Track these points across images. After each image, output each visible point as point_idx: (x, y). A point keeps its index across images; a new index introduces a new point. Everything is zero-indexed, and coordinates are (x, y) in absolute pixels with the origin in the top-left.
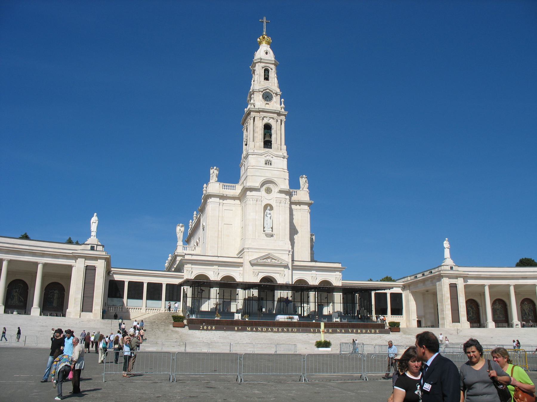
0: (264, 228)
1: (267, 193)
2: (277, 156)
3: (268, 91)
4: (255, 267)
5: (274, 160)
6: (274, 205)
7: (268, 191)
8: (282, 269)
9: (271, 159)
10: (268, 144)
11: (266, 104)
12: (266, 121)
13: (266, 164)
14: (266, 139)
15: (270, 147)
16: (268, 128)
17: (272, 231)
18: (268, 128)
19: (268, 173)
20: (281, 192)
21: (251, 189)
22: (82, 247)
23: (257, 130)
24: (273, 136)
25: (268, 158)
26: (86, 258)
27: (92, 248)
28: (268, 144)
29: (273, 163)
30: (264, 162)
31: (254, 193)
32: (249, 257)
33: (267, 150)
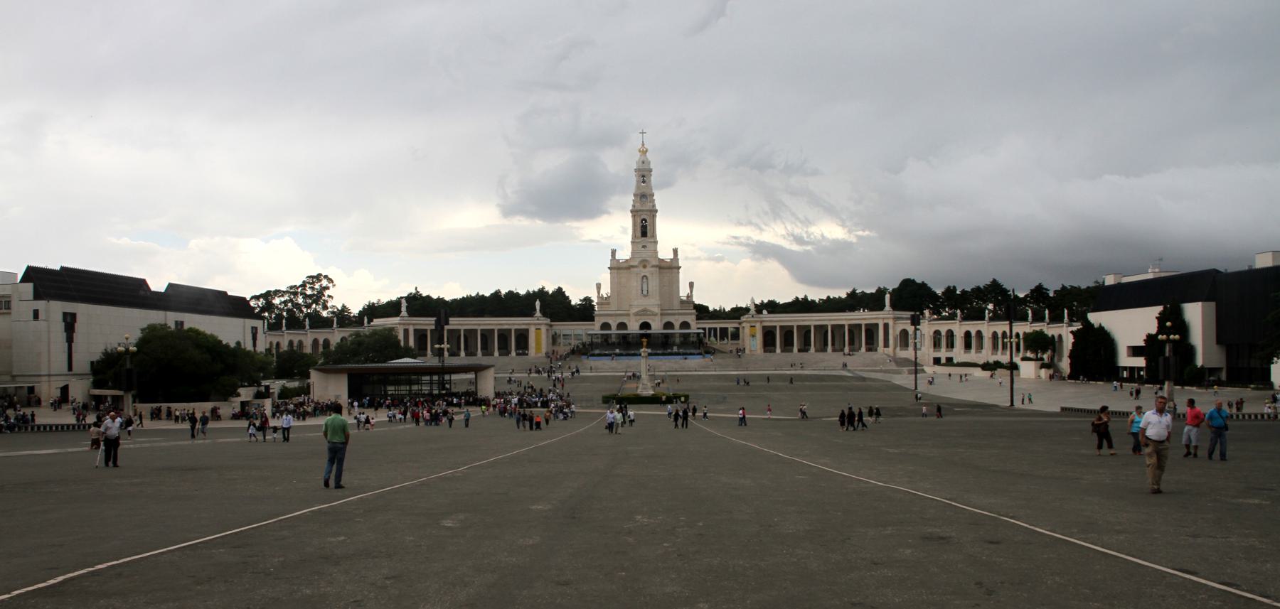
2: (651, 242)
5: (648, 245)
6: (648, 276)
7: (645, 267)
10: (644, 234)
12: (643, 217)
20: (653, 266)
21: (633, 267)
22: (533, 318)
24: (648, 228)
26: (535, 324)
27: (538, 320)
28: (644, 234)
31: (635, 269)
32: (634, 310)
33: (643, 238)
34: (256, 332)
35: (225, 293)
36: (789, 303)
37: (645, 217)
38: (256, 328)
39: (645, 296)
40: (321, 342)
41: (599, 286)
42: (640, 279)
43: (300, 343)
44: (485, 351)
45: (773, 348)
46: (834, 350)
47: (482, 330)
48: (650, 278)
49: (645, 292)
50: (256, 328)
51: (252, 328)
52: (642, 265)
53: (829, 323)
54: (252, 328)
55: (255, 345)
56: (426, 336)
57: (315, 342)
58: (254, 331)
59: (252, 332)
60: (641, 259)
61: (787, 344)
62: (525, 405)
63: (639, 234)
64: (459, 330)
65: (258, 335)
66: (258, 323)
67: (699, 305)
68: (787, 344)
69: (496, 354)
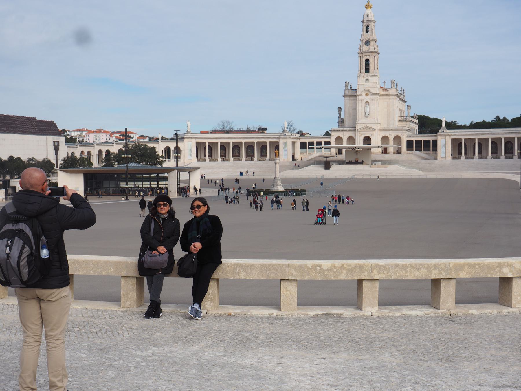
0: (365, 113)
1: (366, 96)
3: (367, 40)
4: (360, 132)
5: (370, 78)
6: (369, 102)
7: (367, 95)
8: (373, 132)
9: (367, 78)
10: (367, 70)
11: (367, 47)
13: (366, 81)
14: (367, 67)
15: (369, 72)
16: (367, 60)
17: (369, 115)
18: (367, 60)
19: (367, 86)
23: (362, 63)
25: (367, 78)
28: (367, 70)
29: (369, 80)
30: (365, 80)
31: (360, 97)
34: (58, 145)
35: (34, 119)
36: (480, 122)
37: (368, 57)
38: (58, 142)
39: (367, 117)
40: (104, 153)
41: (340, 109)
42: (364, 104)
43: (89, 153)
44: (210, 158)
45: (239, 158)
46: (466, 158)
47: (221, 143)
48: (371, 104)
49: (367, 114)
50: (58, 142)
51: (54, 142)
52: (366, 92)
53: (476, 137)
54: (54, 142)
55: (57, 153)
56: (266, 146)
57: (82, 153)
58: (56, 145)
59: (54, 145)
60: (364, 89)
61: (250, 154)
62: (237, 197)
63: (364, 70)
64: (205, 143)
65: (60, 147)
66: (62, 139)
67: (477, 123)
68: (237, 154)
69: (219, 159)
